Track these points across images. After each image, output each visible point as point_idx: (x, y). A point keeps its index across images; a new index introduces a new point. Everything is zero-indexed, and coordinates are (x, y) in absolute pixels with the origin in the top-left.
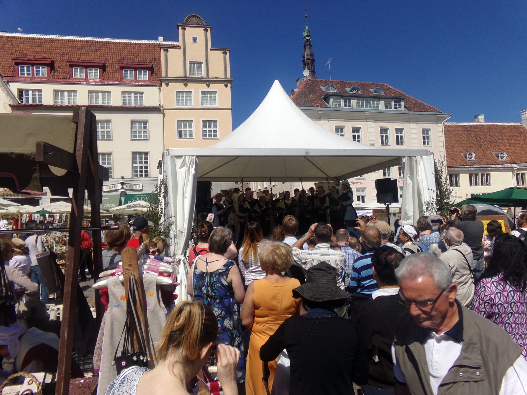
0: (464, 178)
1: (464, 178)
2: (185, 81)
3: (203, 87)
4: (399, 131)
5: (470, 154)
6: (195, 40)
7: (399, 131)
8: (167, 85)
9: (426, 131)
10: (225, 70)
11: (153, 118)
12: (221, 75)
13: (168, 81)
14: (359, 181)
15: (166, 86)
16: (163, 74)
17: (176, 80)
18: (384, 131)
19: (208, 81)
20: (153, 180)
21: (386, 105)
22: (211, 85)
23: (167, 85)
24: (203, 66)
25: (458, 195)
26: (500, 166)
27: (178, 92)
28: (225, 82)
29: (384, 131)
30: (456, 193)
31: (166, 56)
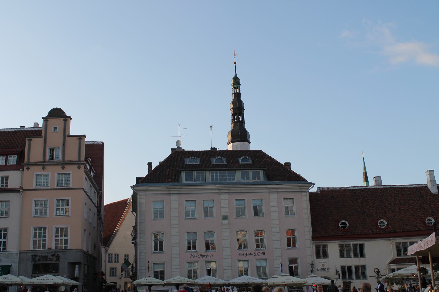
2: (43, 164)
3: (58, 170)
6: (55, 128)
8: (28, 169)
10: (79, 154)
11: (13, 198)
13: (30, 165)
14: (209, 254)
15: (26, 170)
16: (26, 160)
17: (36, 164)
19: (63, 164)
20: (9, 254)
22: (66, 166)
23: (28, 169)
27: (37, 175)
28: (78, 164)
30: (323, 265)
31: (30, 145)
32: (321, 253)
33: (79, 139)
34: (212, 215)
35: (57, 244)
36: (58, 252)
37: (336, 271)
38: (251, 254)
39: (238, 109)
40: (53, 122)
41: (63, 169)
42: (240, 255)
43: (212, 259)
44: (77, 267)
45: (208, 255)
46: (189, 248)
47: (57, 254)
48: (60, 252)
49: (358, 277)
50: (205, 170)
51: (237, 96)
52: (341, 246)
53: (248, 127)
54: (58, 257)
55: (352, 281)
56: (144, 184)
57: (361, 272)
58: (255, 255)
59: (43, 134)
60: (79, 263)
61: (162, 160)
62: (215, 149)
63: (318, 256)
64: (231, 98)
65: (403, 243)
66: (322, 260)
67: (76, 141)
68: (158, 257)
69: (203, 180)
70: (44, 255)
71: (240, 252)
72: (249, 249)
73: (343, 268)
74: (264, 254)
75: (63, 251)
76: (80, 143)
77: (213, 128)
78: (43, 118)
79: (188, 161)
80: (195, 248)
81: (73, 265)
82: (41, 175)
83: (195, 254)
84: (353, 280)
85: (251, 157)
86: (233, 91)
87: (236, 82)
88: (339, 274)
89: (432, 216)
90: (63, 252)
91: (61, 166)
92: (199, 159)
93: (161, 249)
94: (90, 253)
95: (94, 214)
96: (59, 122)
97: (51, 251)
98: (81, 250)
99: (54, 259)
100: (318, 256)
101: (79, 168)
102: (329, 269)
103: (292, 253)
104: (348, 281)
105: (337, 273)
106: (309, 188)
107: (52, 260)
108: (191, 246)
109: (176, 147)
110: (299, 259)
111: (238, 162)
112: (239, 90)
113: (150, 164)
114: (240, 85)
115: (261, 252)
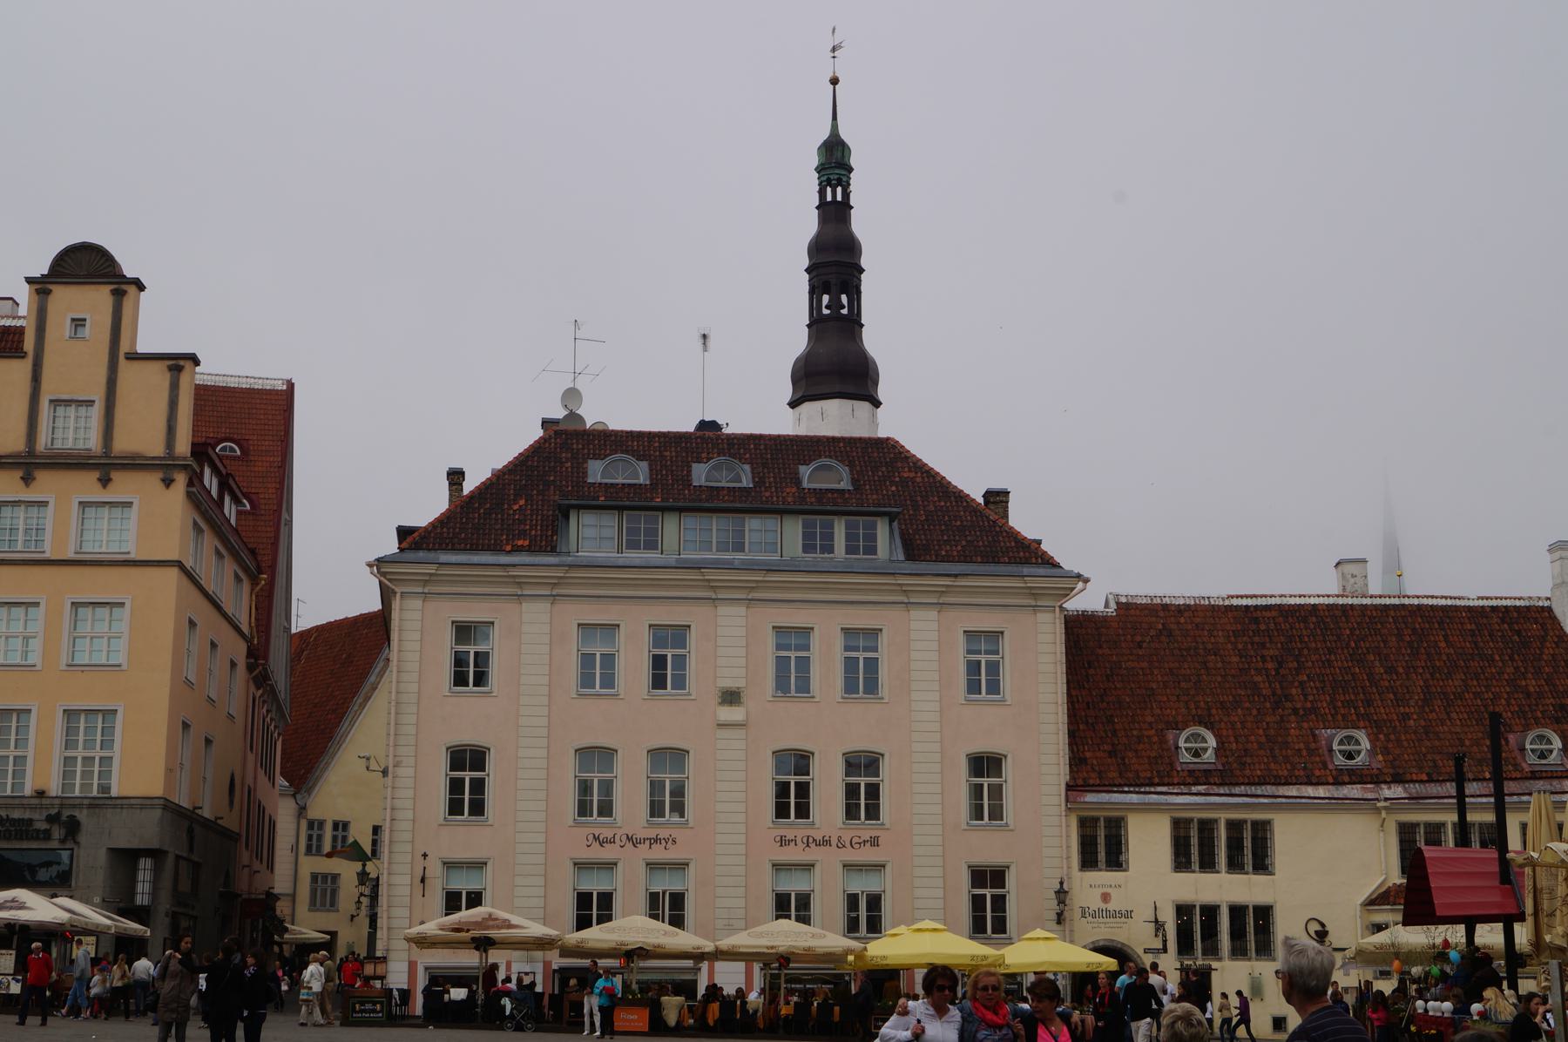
0: (1148, 839)
1: (1148, 839)
3: (85, 485)
4: (861, 639)
5: (1196, 737)
6: (78, 323)
7: (861, 639)
9: (984, 641)
12: (156, 448)
14: (664, 834)
18: (793, 638)
21: (806, 536)
22: (115, 475)
24: (96, 412)
25: (1111, 906)
26: (1321, 791)
28: (165, 468)
29: (793, 638)
30: (1106, 897)
32: (1102, 846)
33: (170, 368)
34: (680, 683)
35: (67, 775)
36: (74, 806)
37: (1156, 921)
38: (826, 842)
39: (835, 265)
40: (69, 300)
41: (104, 486)
42: (783, 841)
43: (672, 854)
44: (145, 864)
45: (657, 840)
46: (583, 809)
47: (66, 813)
48: (80, 806)
49: (1239, 952)
50: (663, 510)
51: (835, 213)
52: (1180, 826)
53: (875, 339)
54: (73, 828)
55: (1215, 965)
56: (421, 554)
57: (1252, 928)
58: (840, 846)
59: (29, 344)
60: (155, 854)
61: (500, 464)
62: (712, 426)
63: (1088, 862)
64: (809, 225)
65: (1428, 825)
66: (1103, 877)
67: (158, 376)
68: (465, 839)
69: (651, 545)
70: (16, 815)
71: (782, 832)
72: (817, 821)
73: (1183, 910)
74: (874, 842)
75: (95, 805)
76: (174, 387)
77: (711, 342)
78: (30, 281)
79: (596, 471)
80: (606, 809)
81: (126, 859)
82: (15, 504)
83: (607, 833)
84: (1220, 959)
85: (851, 465)
86: (822, 193)
87: (835, 162)
88: (1164, 936)
89: (1555, 722)
90: (90, 806)
91: (97, 474)
92: (644, 465)
93: (478, 808)
94: (206, 813)
95: (233, 664)
96: (93, 301)
97: (44, 801)
98: (168, 806)
99: (57, 832)
100: (1088, 861)
101: (168, 482)
102: (1128, 914)
103: (988, 848)
104: (1199, 962)
105: (1157, 930)
106: (1067, 593)
107: (47, 835)
108: (593, 801)
109: (559, 413)
110: (1013, 869)
111: (798, 482)
112: (846, 195)
113: (456, 477)
114: (850, 170)
115: (866, 835)
